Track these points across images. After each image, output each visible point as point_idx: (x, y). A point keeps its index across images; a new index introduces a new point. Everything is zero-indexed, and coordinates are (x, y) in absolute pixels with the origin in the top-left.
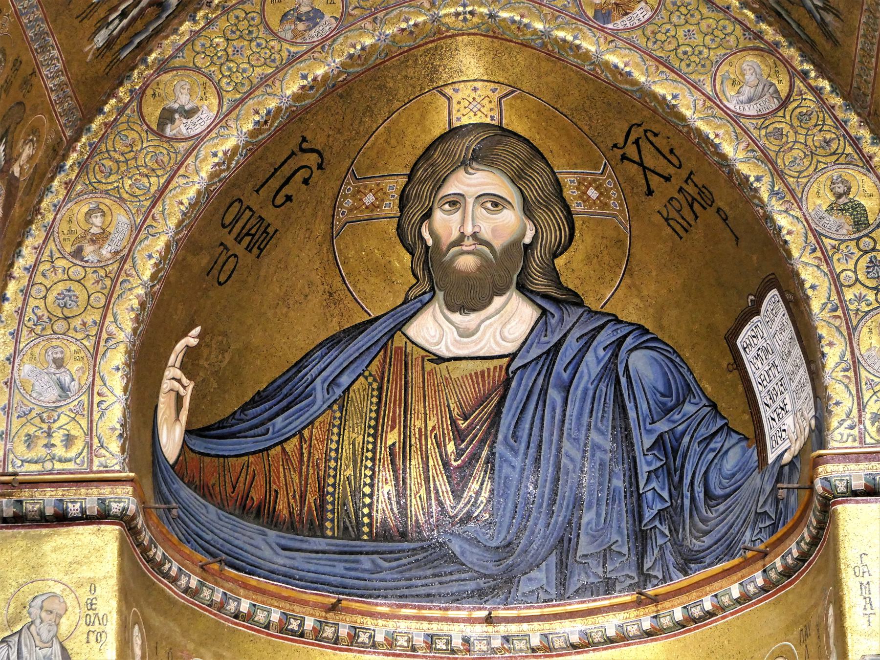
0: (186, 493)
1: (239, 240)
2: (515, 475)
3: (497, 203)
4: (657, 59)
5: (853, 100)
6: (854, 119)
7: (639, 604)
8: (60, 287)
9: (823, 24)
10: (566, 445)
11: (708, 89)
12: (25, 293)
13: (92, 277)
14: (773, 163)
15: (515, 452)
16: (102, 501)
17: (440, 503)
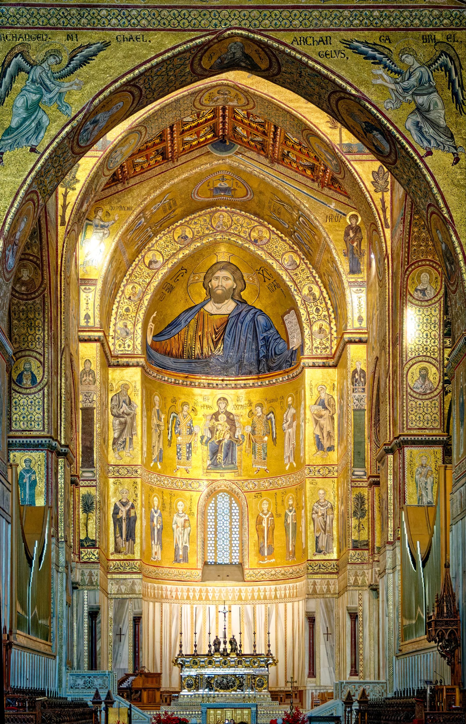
0: (153, 352)
1: (166, 290)
2: (229, 344)
3: (227, 279)
4: (268, 253)
5: (314, 268)
6: (314, 272)
7: (258, 379)
8: (126, 307)
9: (308, 251)
10: (242, 337)
11: (280, 261)
12: (117, 308)
13: (133, 305)
14: (295, 282)
15: (229, 338)
16: (137, 362)
17: (211, 350)
